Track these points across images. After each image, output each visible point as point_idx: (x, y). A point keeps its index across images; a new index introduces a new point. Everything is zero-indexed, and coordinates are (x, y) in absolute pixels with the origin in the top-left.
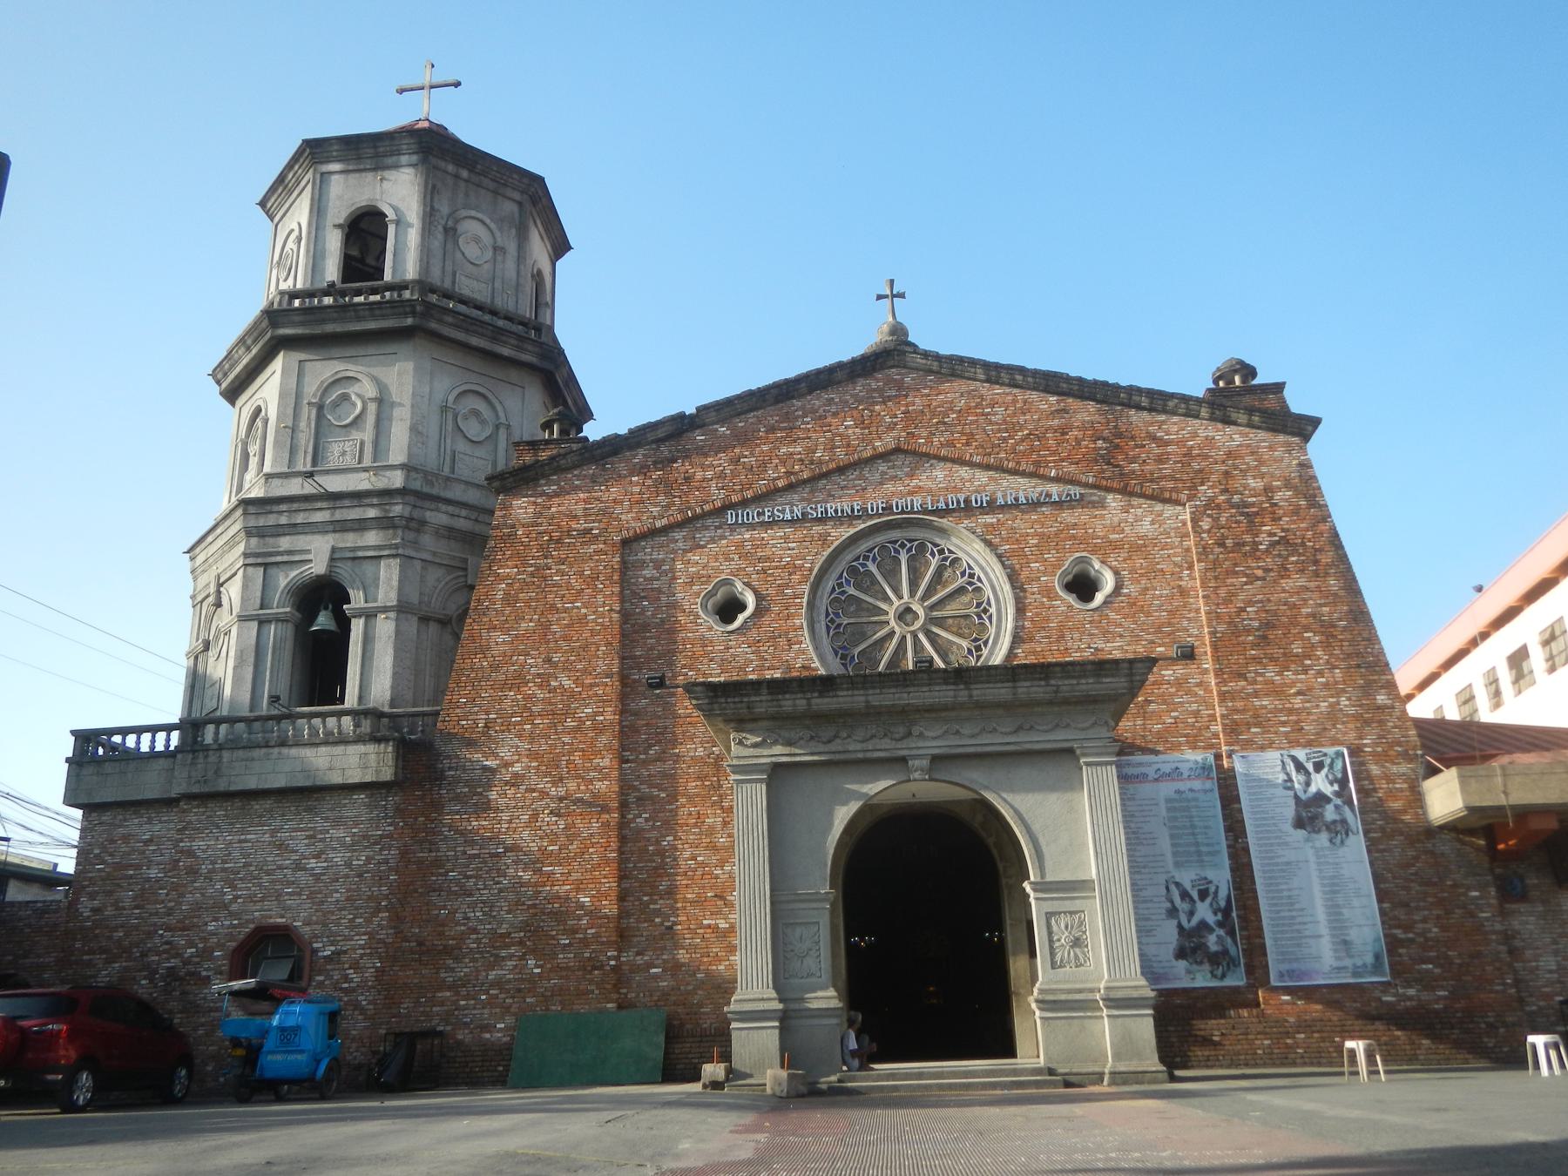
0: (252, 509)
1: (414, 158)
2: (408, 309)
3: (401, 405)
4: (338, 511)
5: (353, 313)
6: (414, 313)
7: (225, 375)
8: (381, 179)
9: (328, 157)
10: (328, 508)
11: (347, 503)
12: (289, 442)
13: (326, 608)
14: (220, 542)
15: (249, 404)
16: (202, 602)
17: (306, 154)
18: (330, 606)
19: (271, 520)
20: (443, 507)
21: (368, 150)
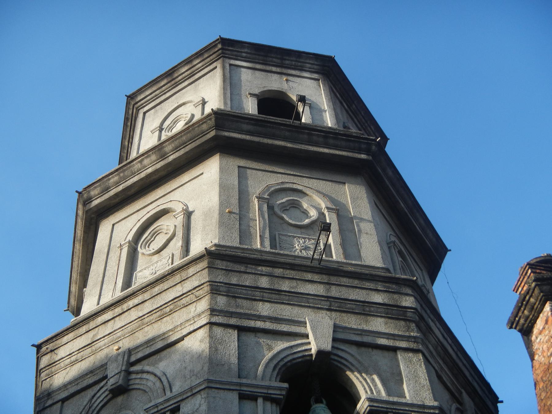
0: (220, 264)
1: (315, 76)
2: (363, 146)
3: (362, 220)
4: (333, 288)
5: (306, 136)
6: (368, 152)
7: (106, 190)
8: (287, 80)
9: (236, 56)
10: (320, 283)
11: (345, 281)
12: (237, 226)
13: (318, 401)
14: (134, 314)
15: (135, 217)
16: (64, 401)
17: (216, 49)
18: (324, 401)
19: (248, 280)
20: (438, 324)
21: (274, 59)
